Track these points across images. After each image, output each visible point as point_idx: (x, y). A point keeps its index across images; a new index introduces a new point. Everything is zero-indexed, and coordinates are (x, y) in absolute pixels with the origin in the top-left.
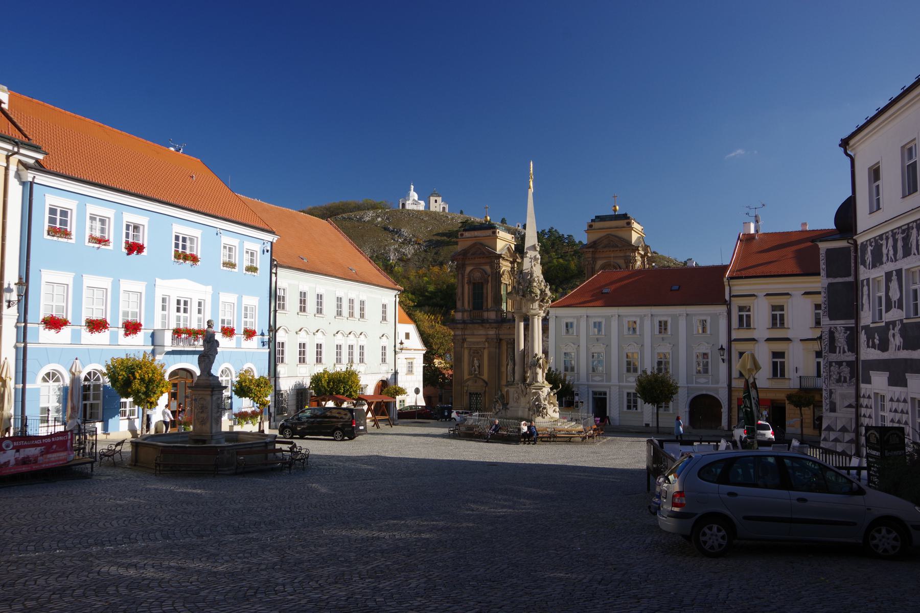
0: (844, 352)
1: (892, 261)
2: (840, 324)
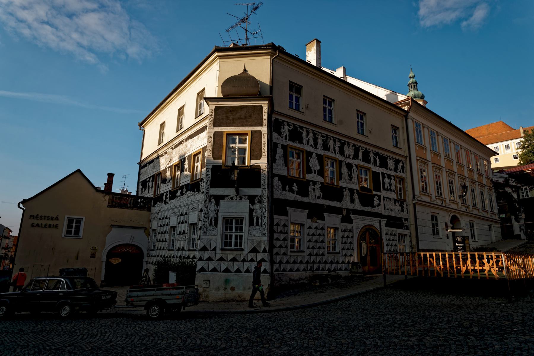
1: (313, 147)
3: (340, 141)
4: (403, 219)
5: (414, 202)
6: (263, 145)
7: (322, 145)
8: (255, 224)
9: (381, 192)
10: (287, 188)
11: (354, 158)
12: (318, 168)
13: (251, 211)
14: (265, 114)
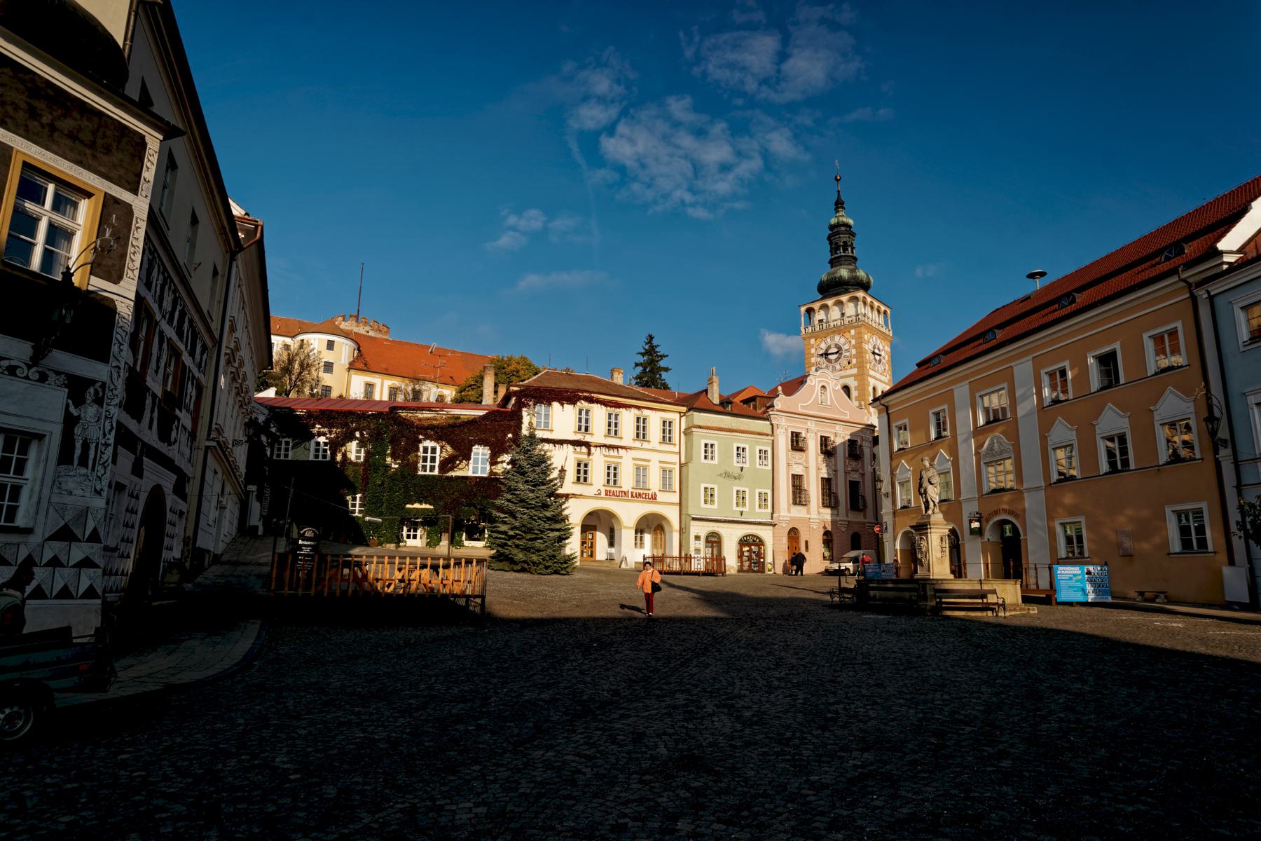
5: (208, 443)
6: (130, 249)
8: (76, 461)
13: (70, 422)
14: (149, 164)
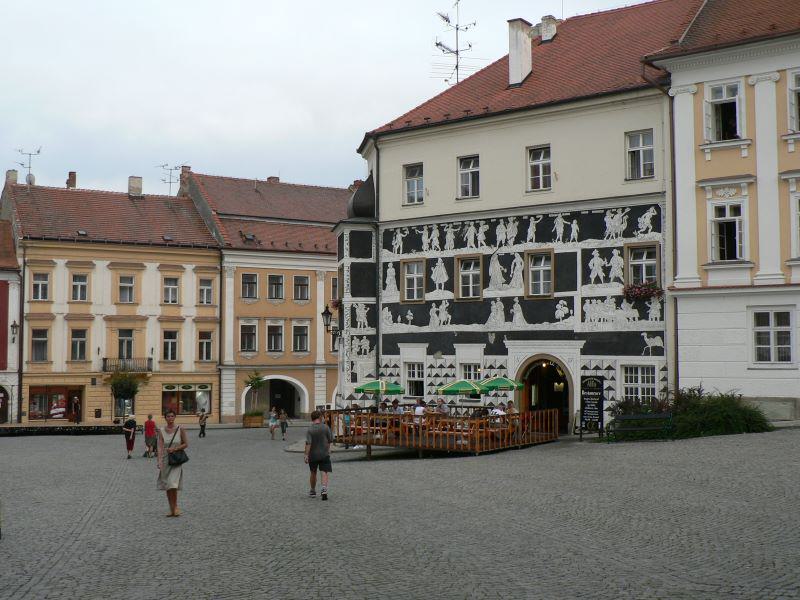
0: (365, 327)
2: (362, 301)
3: (488, 221)
4: (645, 335)
7: (452, 242)
9: (574, 288)
10: (399, 319)
11: (517, 241)
12: (446, 278)
